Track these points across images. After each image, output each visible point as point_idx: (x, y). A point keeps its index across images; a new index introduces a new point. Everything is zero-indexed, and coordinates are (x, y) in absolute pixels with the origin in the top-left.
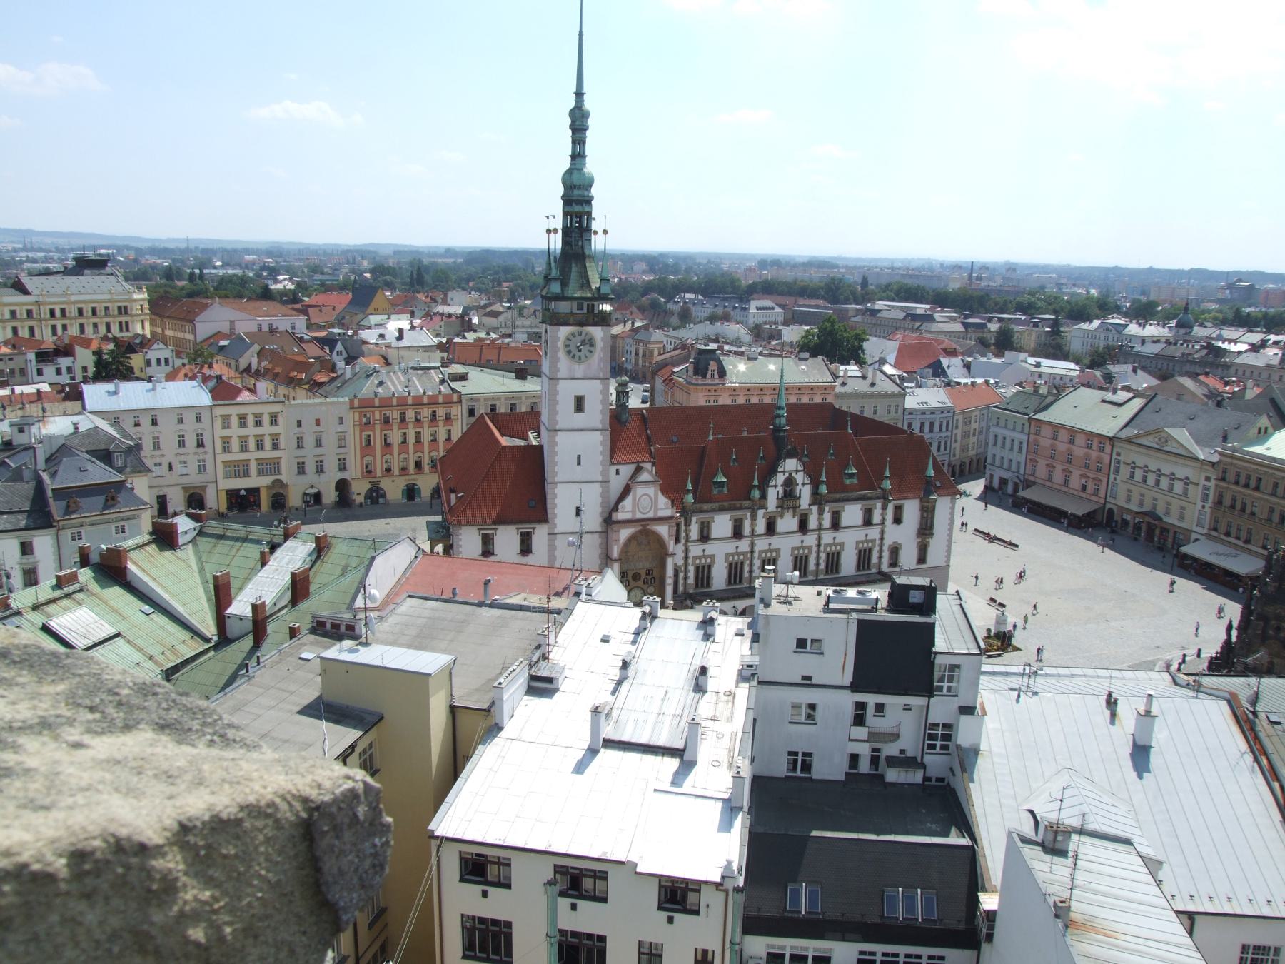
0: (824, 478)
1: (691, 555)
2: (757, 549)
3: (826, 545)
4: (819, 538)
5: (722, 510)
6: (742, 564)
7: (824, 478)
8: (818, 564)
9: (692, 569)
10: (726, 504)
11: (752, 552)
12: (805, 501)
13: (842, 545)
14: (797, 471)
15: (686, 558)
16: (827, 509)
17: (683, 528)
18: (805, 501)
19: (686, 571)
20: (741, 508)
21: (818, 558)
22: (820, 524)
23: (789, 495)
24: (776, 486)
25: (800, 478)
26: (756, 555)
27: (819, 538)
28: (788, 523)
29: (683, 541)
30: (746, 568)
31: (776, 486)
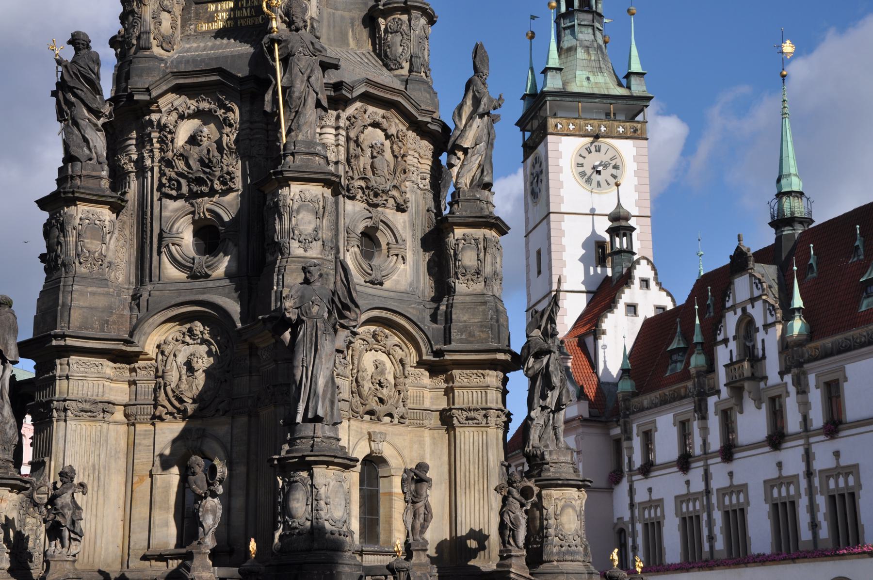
0: (798, 302)
1: (638, 499)
2: (715, 485)
3: (827, 474)
4: (808, 457)
5: (664, 402)
6: (698, 517)
7: (798, 302)
8: (814, 526)
9: (639, 527)
10: (667, 391)
11: (708, 492)
12: (772, 366)
13: (853, 470)
14: (753, 300)
15: (632, 505)
16: (812, 379)
17: (625, 444)
18: (772, 366)
19: (634, 535)
20: (685, 397)
21: (812, 508)
22: (805, 419)
23: (750, 354)
24: (726, 341)
25: (757, 313)
26: (714, 499)
27: (808, 457)
28: (752, 423)
29: (626, 469)
30: (705, 532)
31: (726, 341)
